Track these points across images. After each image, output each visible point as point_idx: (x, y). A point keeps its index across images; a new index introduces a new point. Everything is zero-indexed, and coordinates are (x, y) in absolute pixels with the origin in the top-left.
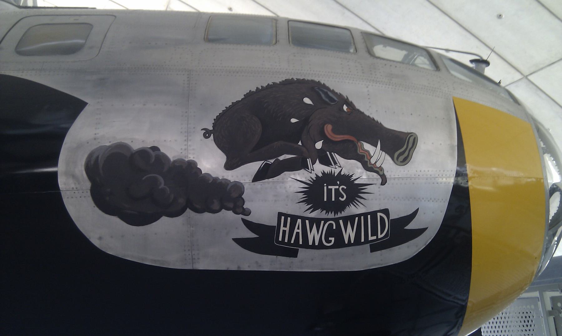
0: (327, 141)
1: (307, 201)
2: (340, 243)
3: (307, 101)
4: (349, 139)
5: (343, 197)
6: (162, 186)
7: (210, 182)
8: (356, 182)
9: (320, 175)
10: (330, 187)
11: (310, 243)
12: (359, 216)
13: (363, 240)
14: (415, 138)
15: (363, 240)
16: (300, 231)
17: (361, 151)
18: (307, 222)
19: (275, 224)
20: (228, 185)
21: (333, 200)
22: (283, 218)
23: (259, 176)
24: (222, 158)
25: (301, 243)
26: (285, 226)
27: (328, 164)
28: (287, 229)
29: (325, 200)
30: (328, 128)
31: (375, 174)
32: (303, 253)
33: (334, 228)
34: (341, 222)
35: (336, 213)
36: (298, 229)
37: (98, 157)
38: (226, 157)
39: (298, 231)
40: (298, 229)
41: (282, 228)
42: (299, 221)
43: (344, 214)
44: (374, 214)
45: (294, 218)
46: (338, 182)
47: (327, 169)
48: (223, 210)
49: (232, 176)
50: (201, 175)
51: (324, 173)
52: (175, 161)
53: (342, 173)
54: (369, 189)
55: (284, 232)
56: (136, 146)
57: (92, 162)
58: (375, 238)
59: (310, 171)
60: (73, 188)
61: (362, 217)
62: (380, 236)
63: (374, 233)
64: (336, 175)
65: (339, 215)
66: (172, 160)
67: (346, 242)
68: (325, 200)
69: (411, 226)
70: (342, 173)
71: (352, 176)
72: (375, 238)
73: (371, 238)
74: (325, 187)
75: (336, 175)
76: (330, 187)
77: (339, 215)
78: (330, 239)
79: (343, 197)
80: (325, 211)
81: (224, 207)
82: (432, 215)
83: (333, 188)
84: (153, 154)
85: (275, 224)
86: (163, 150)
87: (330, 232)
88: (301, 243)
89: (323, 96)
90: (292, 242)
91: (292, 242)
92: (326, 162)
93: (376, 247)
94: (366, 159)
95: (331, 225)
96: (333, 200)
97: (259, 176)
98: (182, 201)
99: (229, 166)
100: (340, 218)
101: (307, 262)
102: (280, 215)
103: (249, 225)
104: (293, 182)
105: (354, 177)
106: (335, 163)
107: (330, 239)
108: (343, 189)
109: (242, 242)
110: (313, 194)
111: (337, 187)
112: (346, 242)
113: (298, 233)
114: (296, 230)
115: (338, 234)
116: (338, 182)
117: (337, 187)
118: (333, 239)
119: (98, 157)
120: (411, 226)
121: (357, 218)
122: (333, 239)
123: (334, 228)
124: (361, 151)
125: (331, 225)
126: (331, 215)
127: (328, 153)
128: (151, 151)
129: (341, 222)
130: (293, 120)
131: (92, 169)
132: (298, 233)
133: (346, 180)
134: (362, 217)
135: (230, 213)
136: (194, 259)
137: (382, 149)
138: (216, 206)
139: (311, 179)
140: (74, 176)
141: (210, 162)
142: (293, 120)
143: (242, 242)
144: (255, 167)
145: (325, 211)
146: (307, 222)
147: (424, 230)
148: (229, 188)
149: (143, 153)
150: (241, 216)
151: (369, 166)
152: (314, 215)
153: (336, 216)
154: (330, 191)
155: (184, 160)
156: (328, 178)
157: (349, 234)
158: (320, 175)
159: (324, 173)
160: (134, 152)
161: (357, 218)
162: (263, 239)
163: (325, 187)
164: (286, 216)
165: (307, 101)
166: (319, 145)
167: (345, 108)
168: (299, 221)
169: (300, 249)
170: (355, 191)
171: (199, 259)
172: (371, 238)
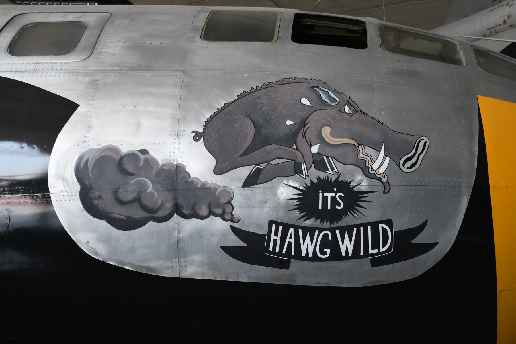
1: (300, 209)
2: (336, 255)
3: (305, 101)
4: (349, 142)
5: (339, 205)
6: (150, 189)
7: (199, 186)
8: (355, 189)
9: (315, 181)
10: (325, 194)
11: (304, 254)
12: (358, 226)
13: (362, 253)
14: (426, 142)
15: (362, 253)
16: (292, 241)
17: (362, 156)
18: (300, 231)
19: (265, 232)
20: (217, 189)
21: (329, 208)
22: (274, 226)
23: (250, 181)
24: (211, 161)
25: (293, 253)
26: (276, 234)
27: (324, 169)
28: (278, 238)
29: (320, 208)
30: (326, 132)
31: (377, 182)
32: (295, 265)
33: (330, 238)
34: (337, 232)
35: (332, 222)
36: (290, 238)
37: (88, 160)
38: (215, 161)
39: (290, 240)
40: (290, 238)
41: (273, 237)
42: (291, 230)
43: (341, 224)
44: (375, 225)
45: (286, 227)
46: (335, 189)
47: (323, 175)
48: (211, 216)
49: (219, 181)
50: (190, 180)
51: (319, 179)
52: (163, 165)
53: (340, 179)
54: (368, 197)
55: (275, 241)
56: (125, 149)
57: (82, 165)
58: (376, 251)
59: (304, 177)
60: (62, 191)
61: (362, 228)
62: (382, 250)
63: (376, 245)
64: (333, 181)
65: (336, 225)
66: (161, 163)
67: (344, 255)
68: (320, 208)
69: (419, 240)
70: (340, 179)
71: (350, 183)
72: (376, 251)
73: (371, 251)
74: (321, 195)
75: (333, 181)
76: (325, 194)
77: (336, 225)
78: (325, 250)
79: (339, 205)
80: (319, 220)
81: (211, 213)
83: (329, 195)
84: (142, 157)
85: (265, 232)
86: (152, 153)
87: (325, 243)
88: (293, 253)
89: (323, 96)
90: (284, 252)
91: (284, 252)
93: (378, 261)
94: (367, 165)
95: (326, 235)
96: (329, 208)
97: (250, 181)
98: (169, 206)
99: (218, 171)
100: (337, 228)
101: (299, 275)
102: (271, 222)
103: (236, 231)
105: (353, 184)
106: (332, 169)
107: (325, 250)
108: (340, 196)
109: (229, 250)
110: (307, 201)
111: (334, 194)
112: (344, 255)
113: (290, 243)
114: (288, 240)
116: (335, 189)
117: (334, 194)
118: (328, 251)
119: (87, 160)
120: (419, 240)
121: (355, 229)
122: (328, 251)
123: (330, 238)
124: (362, 156)
125: (326, 235)
126: (327, 225)
127: (325, 157)
128: (140, 154)
129: (337, 232)
130: (289, 123)
131: (81, 172)
132: (290, 243)
133: (343, 186)
134: (362, 228)
135: (219, 220)
136: (181, 267)
137: (386, 155)
138: (204, 211)
139: (305, 186)
140: (63, 179)
141: (198, 164)
142: (289, 123)
145: (319, 220)
146: (300, 231)
147: (432, 246)
148: (218, 192)
149: (132, 156)
150: (229, 223)
151: (371, 172)
152: (309, 223)
153: (332, 226)
154: (325, 199)
155: (173, 164)
156: (325, 185)
157: (347, 245)
158: (315, 181)
159: (319, 179)
160: (123, 155)
161: (355, 229)
162: (251, 247)
163: (321, 195)
164: (278, 224)
165: (305, 101)
166: (315, 149)
167: (347, 109)
168: (291, 230)
169: (292, 261)
170: (354, 198)
171: (185, 267)
172: (371, 251)
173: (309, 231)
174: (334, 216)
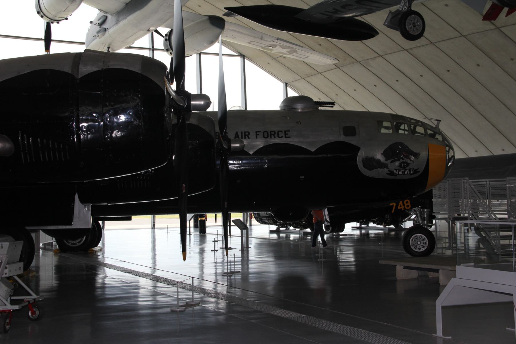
0: (404, 156)
2: (404, 174)
23: (391, 162)
24: (385, 159)
49: (386, 162)
56: (370, 157)
69: (418, 171)
82: (421, 170)
92: (403, 159)
97: (391, 162)
99: (386, 160)
101: (398, 177)
103: (389, 171)
104: (397, 163)
109: (388, 174)
110: (400, 165)
115: (404, 172)
120: (418, 171)
131: (363, 161)
133: (406, 163)
143: (388, 174)
144: (390, 160)
149: (371, 158)
156: (404, 162)
157: (406, 172)
170: (408, 165)
173: (400, 170)
174: (405, 167)
